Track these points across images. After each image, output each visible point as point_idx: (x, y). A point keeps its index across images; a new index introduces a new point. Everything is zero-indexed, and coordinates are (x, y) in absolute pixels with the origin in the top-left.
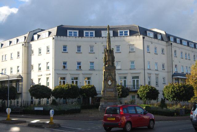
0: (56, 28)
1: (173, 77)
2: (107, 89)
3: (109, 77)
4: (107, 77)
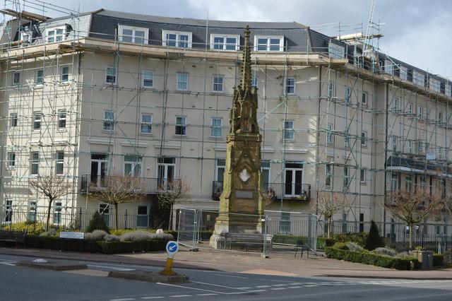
0: (89, 17)
1: (388, 168)
3: (243, 160)
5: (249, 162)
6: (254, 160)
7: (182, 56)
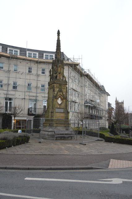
2: (56, 109)
3: (59, 93)
4: (57, 94)
5: (62, 95)
6: (64, 93)
7: (17, 58)
